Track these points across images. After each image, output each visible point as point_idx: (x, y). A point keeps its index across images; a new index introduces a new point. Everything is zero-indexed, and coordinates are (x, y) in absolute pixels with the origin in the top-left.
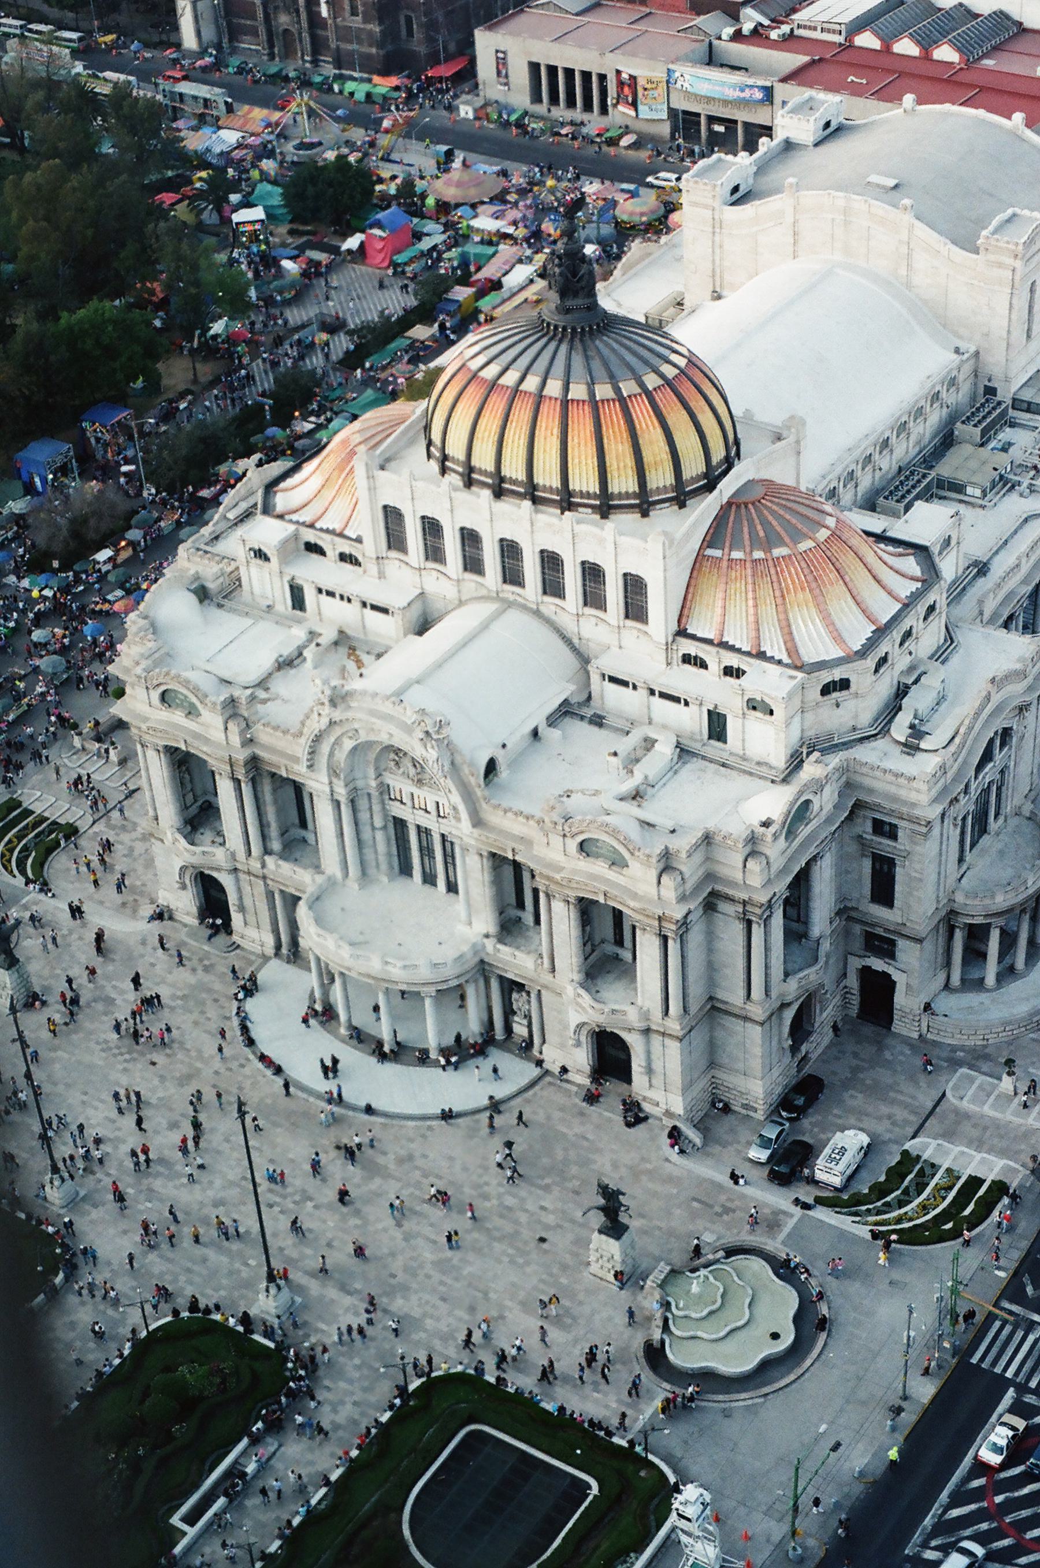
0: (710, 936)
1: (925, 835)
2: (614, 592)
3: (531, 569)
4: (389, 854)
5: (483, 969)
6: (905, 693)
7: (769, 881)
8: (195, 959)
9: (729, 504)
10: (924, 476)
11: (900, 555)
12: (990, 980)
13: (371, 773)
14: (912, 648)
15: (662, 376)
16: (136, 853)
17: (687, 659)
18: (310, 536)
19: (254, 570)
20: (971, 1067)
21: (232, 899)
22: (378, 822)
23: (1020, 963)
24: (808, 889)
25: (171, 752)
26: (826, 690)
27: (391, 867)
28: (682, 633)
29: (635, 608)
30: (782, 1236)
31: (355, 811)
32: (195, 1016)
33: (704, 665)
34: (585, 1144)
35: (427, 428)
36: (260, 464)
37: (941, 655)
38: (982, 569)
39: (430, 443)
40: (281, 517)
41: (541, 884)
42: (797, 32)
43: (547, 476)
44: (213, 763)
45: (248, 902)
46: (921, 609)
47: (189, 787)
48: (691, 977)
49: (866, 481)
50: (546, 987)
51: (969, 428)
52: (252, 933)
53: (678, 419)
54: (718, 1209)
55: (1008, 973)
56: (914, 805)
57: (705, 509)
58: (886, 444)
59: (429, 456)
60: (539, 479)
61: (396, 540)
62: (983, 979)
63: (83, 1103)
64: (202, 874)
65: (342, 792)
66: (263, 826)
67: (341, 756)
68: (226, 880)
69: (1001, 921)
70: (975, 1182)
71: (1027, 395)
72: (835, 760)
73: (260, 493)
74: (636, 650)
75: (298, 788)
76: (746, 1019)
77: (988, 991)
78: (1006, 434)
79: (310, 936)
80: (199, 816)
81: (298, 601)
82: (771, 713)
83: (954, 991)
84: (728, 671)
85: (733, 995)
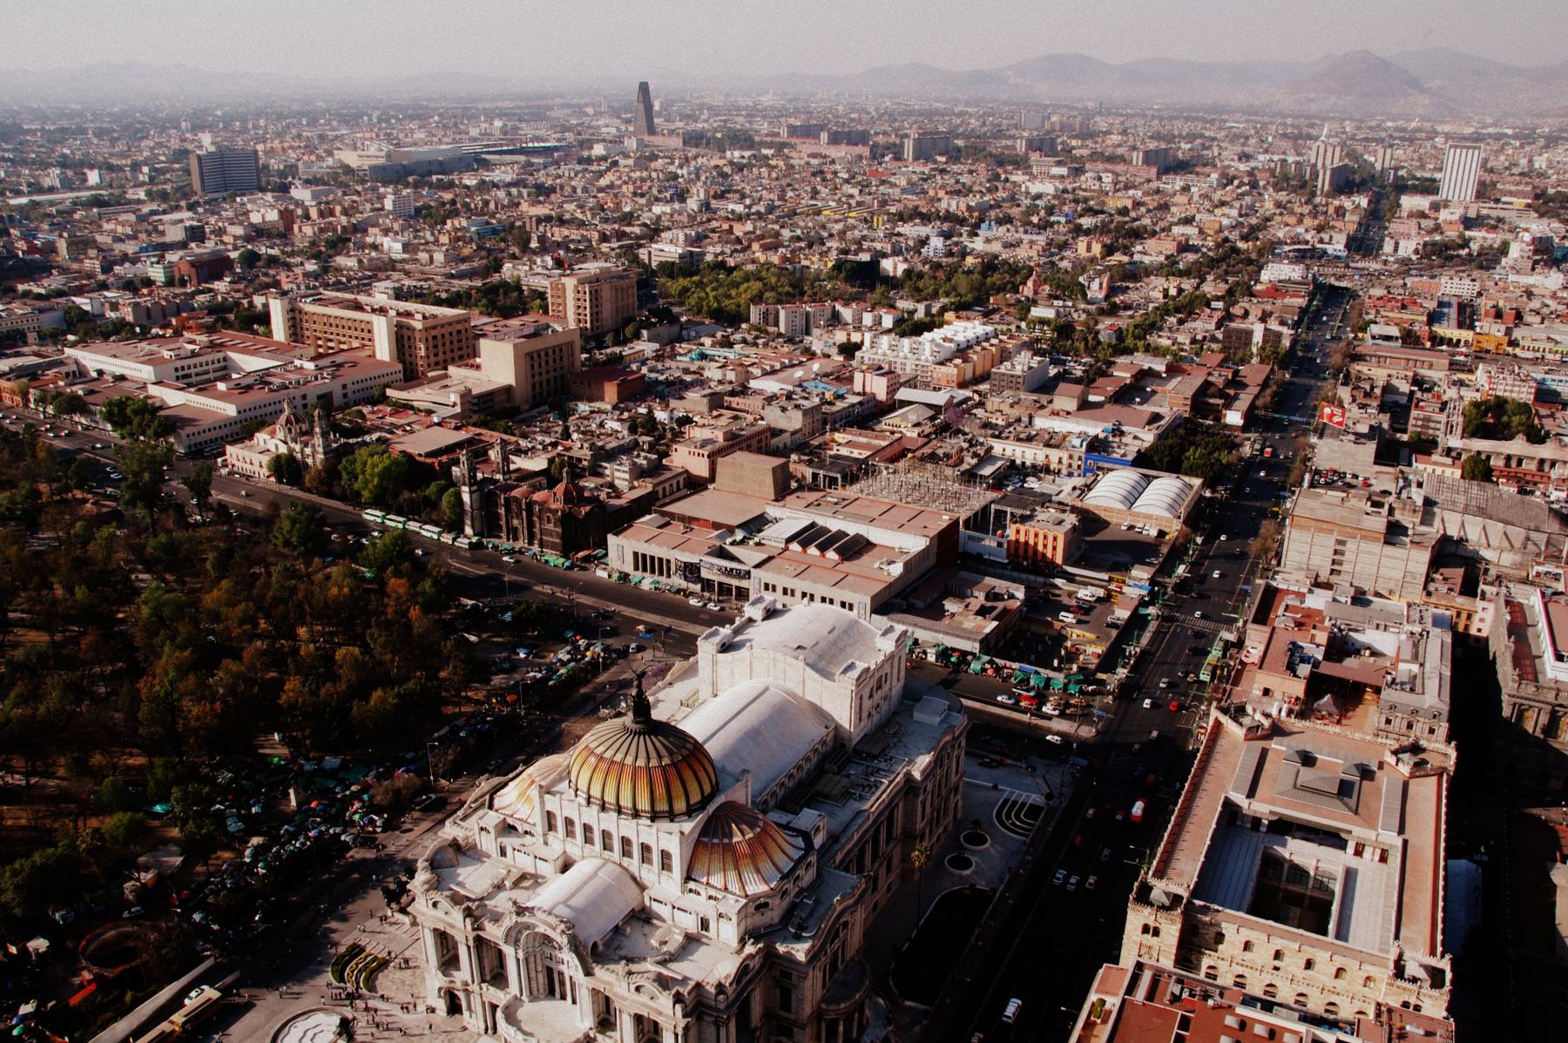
18: (510, 821)
25: (435, 930)
29: (666, 864)
43: (626, 802)
49: (781, 793)
57: (701, 818)
60: (622, 803)
61: (551, 826)
65: (521, 955)
68: (461, 995)
75: (500, 951)
80: (449, 962)
81: (503, 853)
84: (710, 897)
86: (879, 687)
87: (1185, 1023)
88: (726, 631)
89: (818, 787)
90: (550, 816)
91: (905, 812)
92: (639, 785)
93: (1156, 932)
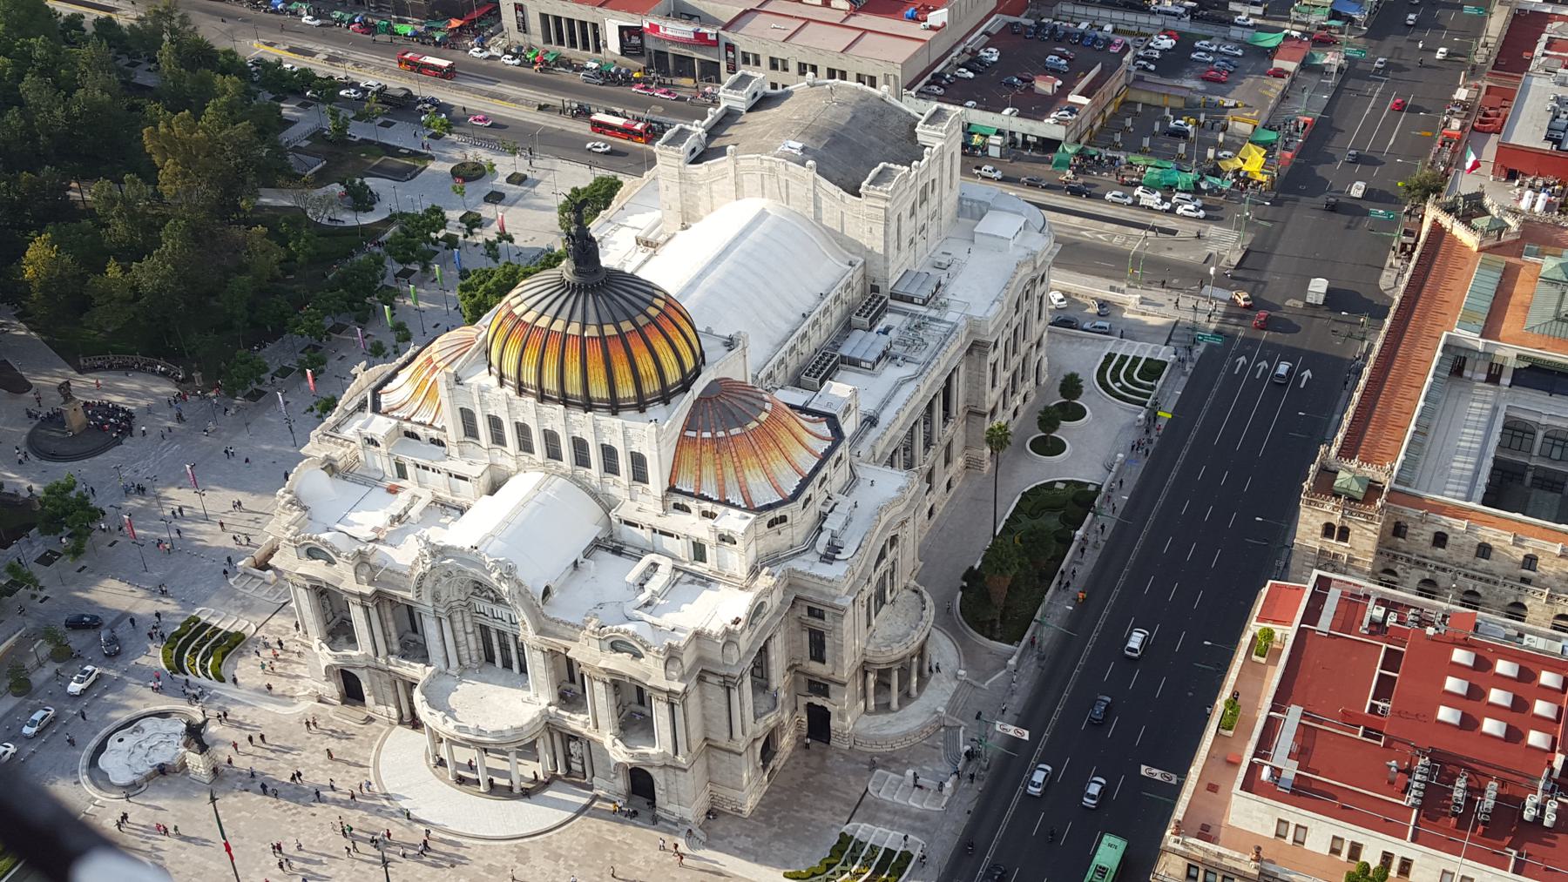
2: (624, 464)
3: (566, 449)
12: (895, 705)
15: (648, 316)
17: (676, 506)
18: (408, 426)
20: (884, 767)
22: (469, 630)
23: (914, 692)
24: (767, 657)
26: (771, 524)
28: (672, 489)
29: (640, 474)
31: (451, 622)
33: (688, 510)
35: (488, 352)
37: (847, 489)
39: (490, 365)
40: (385, 413)
41: (587, 672)
48: (691, 729)
49: (793, 363)
51: (861, 319)
53: (660, 345)
55: (906, 697)
56: (834, 597)
57: (684, 404)
58: (805, 335)
60: (569, 391)
61: (470, 430)
62: (888, 704)
70: (889, 853)
71: (901, 290)
72: (779, 570)
74: (643, 506)
75: (410, 609)
78: (888, 319)
79: (423, 710)
80: (338, 631)
83: (870, 714)
84: (705, 514)
86: (924, 199)
87: (1392, 660)
89: (845, 351)
90: (468, 418)
91: (969, 379)
92: (590, 365)
93: (1344, 534)
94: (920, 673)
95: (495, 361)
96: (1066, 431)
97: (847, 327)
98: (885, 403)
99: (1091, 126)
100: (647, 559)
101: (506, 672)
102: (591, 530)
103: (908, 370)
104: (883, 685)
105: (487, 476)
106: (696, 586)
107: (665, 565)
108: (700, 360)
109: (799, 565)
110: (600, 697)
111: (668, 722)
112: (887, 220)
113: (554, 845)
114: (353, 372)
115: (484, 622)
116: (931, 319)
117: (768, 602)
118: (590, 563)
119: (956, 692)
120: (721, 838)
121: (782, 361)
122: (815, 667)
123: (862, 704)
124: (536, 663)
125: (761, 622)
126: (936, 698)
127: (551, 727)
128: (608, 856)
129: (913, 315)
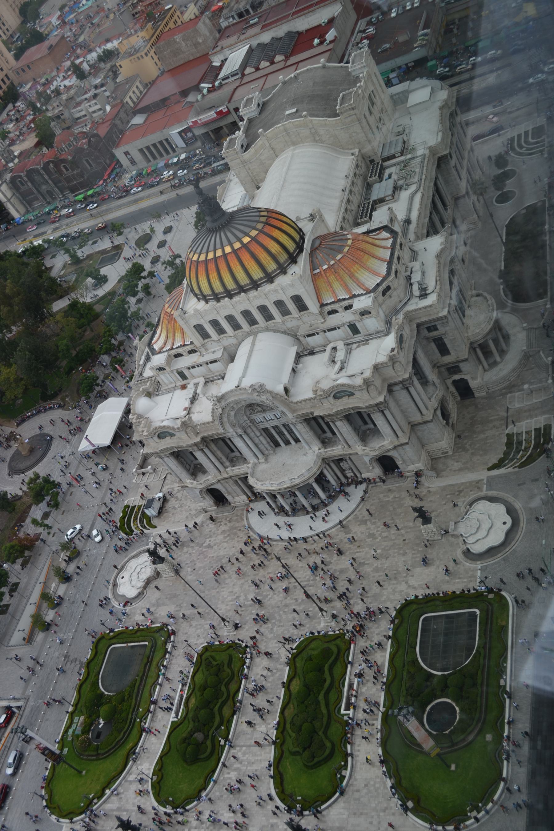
0: (396, 401)
1: (447, 322)
2: (291, 306)
4: (268, 443)
5: (325, 461)
6: (410, 279)
7: (405, 370)
8: (223, 520)
9: (311, 252)
10: (369, 203)
11: (378, 234)
12: (498, 359)
13: (246, 418)
14: (403, 262)
15: (262, 222)
16: (179, 497)
17: (330, 313)
18: (174, 352)
19: (162, 376)
20: (510, 392)
21: (223, 490)
22: (258, 434)
24: (419, 365)
26: (384, 294)
27: (272, 447)
28: (322, 305)
29: (302, 306)
30: (484, 489)
31: (248, 435)
32: (236, 539)
34: (397, 499)
35: (192, 290)
36: (140, 340)
38: (408, 222)
39: (196, 295)
40: (160, 352)
41: (327, 419)
42: (224, 82)
44: (190, 449)
45: (230, 489)
46: (398, 247)
47: (185, 462)
48: (399, 420)
49: (350, 218)
50: (351, 454)
52: (237, 499)
54: (457, 493)
55: (502, 353)
57: (303, 259)
58: (348, 201)
59: (199, 300)
60: (242, 284)
61: (205, 335)
63: (218, 592)
64: (208, 490)
65: (240, 431)
66: (219, 460)
67: (232, 418)
68: (218, 487)
69: (490, 337)
70: (537, 430)
71: (386, 154)
72: (401, 316)
73: (147, 349)
75: (223, 440)
76: (426, 422)
77: (499, 363)
78: (387, 172)
79: (259, 486)
80: (195, 470)
81: (184, 377)
82: (370, 313)
83: (488, 370)
85: (417, 418)
86: (373, 104)
88: (239, 134)
89: (374, 196)
90: (199, 328)
92: (246, 263)
94: (504, 337)
95: (197, 291)
96: (510, 185)
97: (369, 187)
98: (410, 210)
99: (438, 43)
100: (329, 348)
101: (289, 447)
102: (293, 351)
103: (413, 188)
104: (487, 353)
105: (226, 354)
106: (362, 347)
107: (340, 345)
108: (300, 231)
109: (411, 307)
110: (343, 428)
111: (385, 422)
112: (359, 120)
113: (360, 517)
114: (134, 344)
115: (263, 427)
116: (410, 159)
117: (403, 332)
118: (300, 366)
119: (528, 336)
120: (444, 470)
121: (344, 218)
122: (447, 359)
123: (481, 367)
124: (302, 431)
125: (405, 345)
126: (519, 340)
127: (325, 461)
128: (391, 508)
129: (399, 163)
